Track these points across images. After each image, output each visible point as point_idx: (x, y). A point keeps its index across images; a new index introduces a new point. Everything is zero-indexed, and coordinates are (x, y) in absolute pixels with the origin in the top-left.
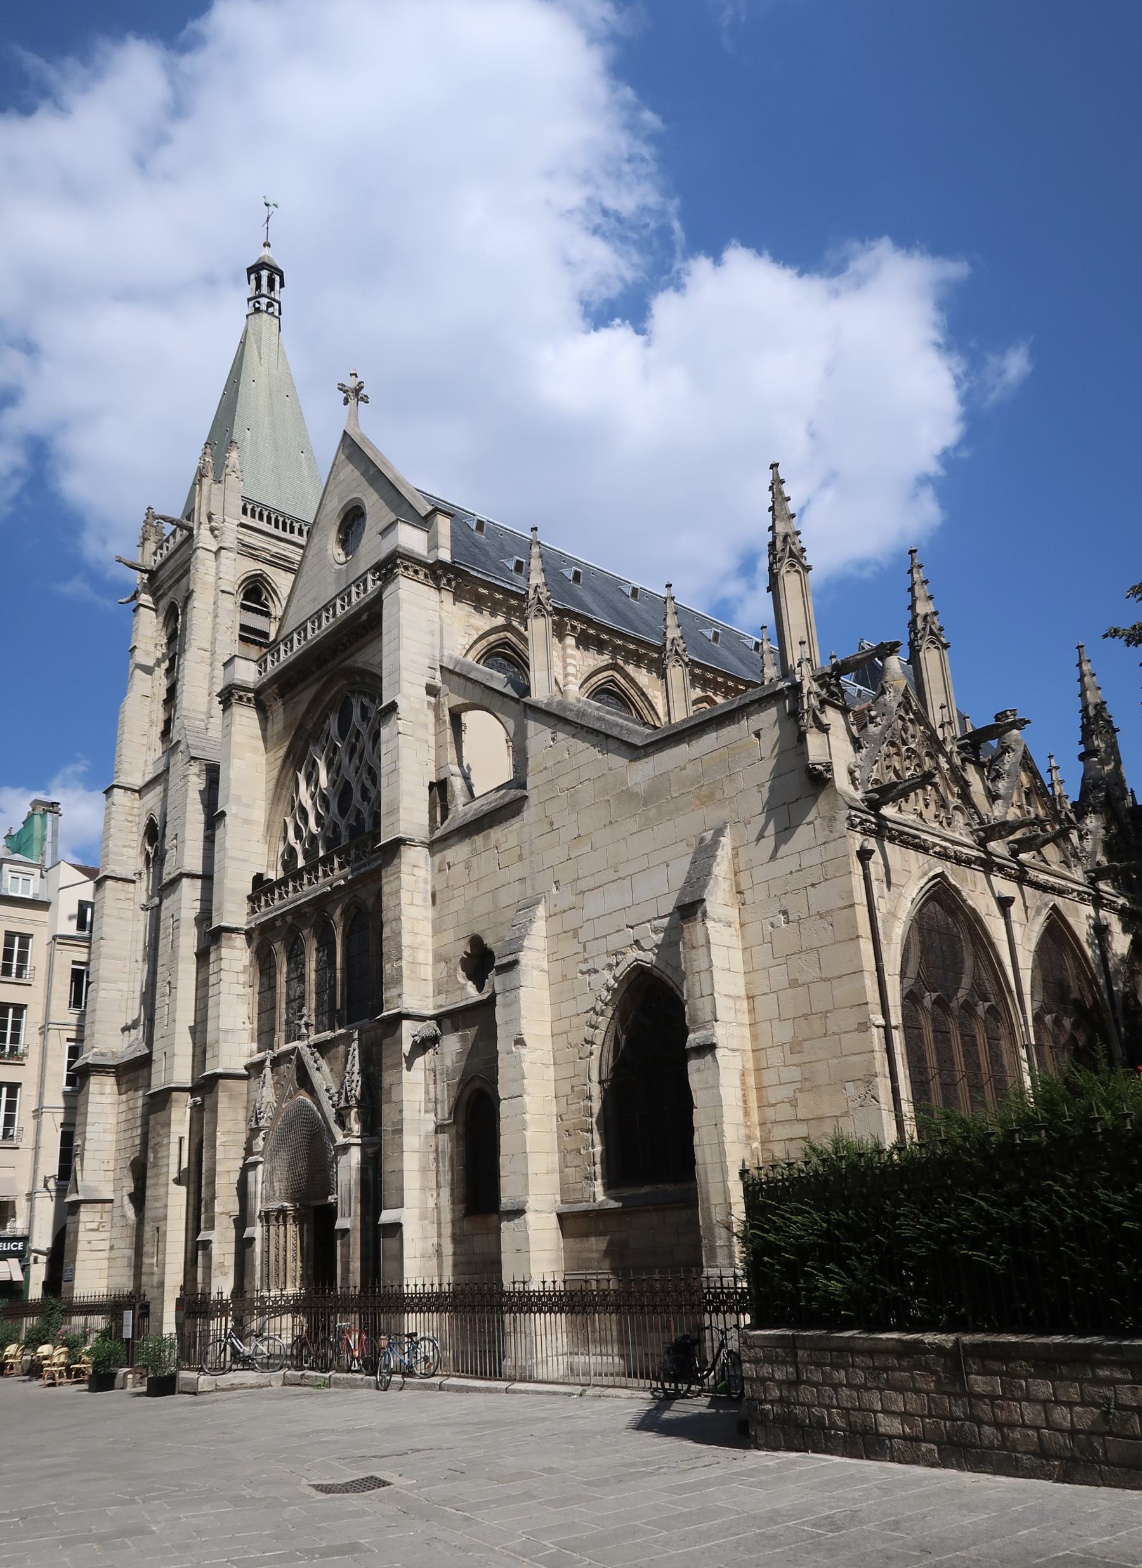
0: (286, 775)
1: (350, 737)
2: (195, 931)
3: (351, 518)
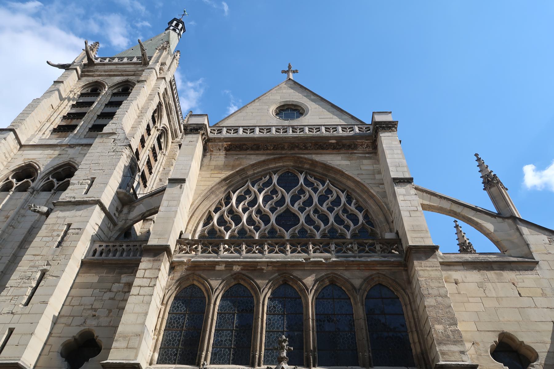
0: (219, 188)
1: (296, 190)
2: (88, 244)
3: (286, 107)
